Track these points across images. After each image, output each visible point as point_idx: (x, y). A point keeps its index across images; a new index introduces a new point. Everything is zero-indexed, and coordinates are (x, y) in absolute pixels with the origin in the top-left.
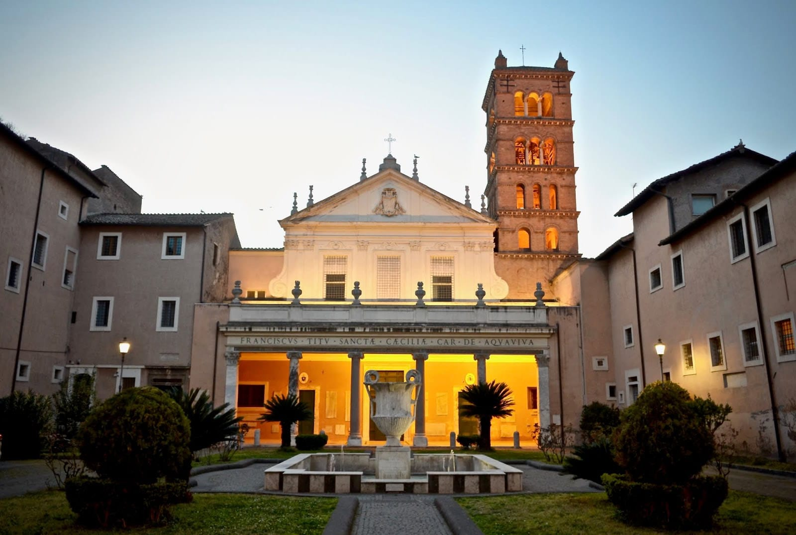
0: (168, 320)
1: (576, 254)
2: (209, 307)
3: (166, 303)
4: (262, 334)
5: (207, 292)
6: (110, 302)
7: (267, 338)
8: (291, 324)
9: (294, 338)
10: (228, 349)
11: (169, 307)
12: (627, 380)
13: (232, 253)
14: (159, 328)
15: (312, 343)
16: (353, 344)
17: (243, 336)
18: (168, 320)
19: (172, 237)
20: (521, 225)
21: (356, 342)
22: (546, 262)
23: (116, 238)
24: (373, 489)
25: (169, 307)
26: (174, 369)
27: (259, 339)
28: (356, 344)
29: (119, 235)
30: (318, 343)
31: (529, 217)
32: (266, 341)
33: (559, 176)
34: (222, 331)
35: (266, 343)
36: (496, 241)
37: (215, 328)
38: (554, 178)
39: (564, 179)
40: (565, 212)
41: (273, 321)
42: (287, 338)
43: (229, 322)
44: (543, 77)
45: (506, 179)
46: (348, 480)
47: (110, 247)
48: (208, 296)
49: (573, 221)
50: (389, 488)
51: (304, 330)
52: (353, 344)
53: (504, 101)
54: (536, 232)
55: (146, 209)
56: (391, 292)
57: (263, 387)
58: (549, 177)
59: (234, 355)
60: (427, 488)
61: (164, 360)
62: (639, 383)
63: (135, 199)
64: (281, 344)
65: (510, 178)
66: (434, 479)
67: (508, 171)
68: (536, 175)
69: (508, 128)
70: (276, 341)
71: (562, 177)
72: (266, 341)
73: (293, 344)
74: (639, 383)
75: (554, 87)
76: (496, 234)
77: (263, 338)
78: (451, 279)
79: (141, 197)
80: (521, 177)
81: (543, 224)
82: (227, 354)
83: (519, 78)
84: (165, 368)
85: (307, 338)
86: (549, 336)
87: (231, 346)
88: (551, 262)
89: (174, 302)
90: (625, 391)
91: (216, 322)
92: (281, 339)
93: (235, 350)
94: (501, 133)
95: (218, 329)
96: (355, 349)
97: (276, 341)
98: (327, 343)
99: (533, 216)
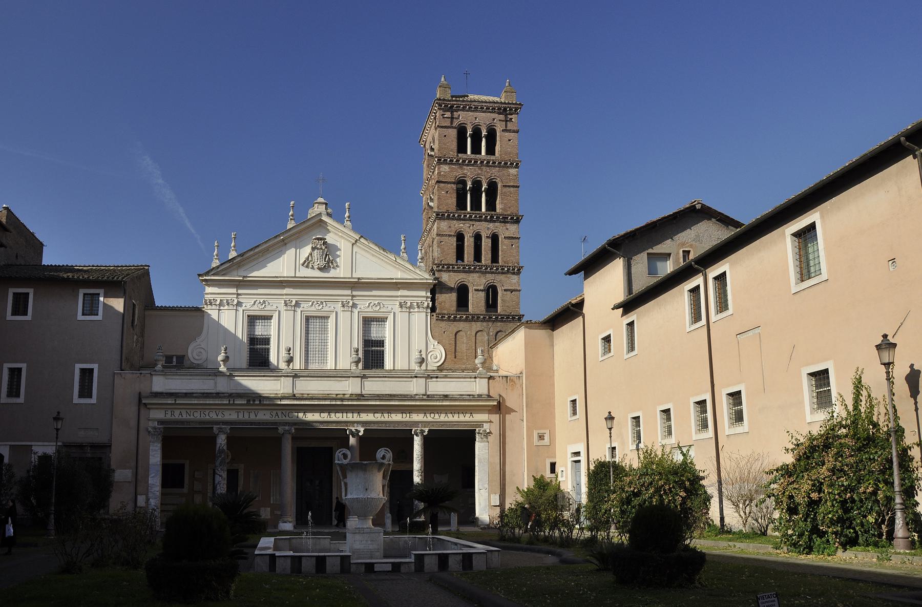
0: (85, 391)
1: (517, 316)
2: (129, 374)
3: (83, 371)
4: (188, 407)
5: (126, 358)
6: (23, 369)
7: (192, 411)
8: (218, 395)
9: (221, 411)
10: (151, 424)
11: (87, 374)
12: (569, 455)
13: (147, 313)
14: (76, 400)
15: (241, 417)
16: (284, 418)
17: (167, 408)
18: (85, 391)
19: (87, 294)
20: (458, 282)
21: (287, 416)
22: (485, 324)
23: (28, 294)
24: (363, 569)
25: (87, 374)
26: (94, 446)
27: (184, 412)
28: (287, 418)
29: (31, 291)
30: (246, 417)
31: (469, 272)
32: (192, 414)
33: (503, 224)
34: (145, 404)
35: (192, 417)
36: (433, 300)
37: (137, 400)
38: (497, 227)
39: (507, 229)
40: (507, 267)
41: (199, 391)
42: (214, 411)
43: (151, 393)
44: (489, 109)
45: (445, 228)
46: (338, 560)
47: (20, 306)
48: (127, 362)
49: (515, 277)
50: (377, 568)
51: (231, 402)
52: (284, 418)
53: (445, 136)
54: (476, 290)
55: (49, 258)
56: (320, 359)
57: (183, 466)
58: (491, 225)
59: (158, 430)
60: (413, 568)
61: (82, 436)
62: (583, 458)
63: (37, 247)
64: (207, 417)
65: (450, 227)
66: (420, 558)
67: (448, 218)
68: (478, 223)
69: (449, 168)
70: (202, 415)
71: (505, 226)
72: (192, 414)
73: (220, 417)
74: (583, 458)
75: (500, 120)
76: (433, 292)
77: (188, 411)
78: (383, 343)
79: (41, 245)
80: (462, 225)
81: (485, 281)
82: (150, 429)
83: (464, 109)
84: (84, 444)
85: (235, 411)
86: (491, 408)
87: (153, 420)
88: (490, 324)
89: (92, 370)
90: (566, 468)
91: (138, 392)
92: (207, 412)
93: (158, 425)
94: (442, 173)
95: (140, 400)
96: (286, 423)
97: (202, 415)
98: (256, 416)
99: (472, 272)
